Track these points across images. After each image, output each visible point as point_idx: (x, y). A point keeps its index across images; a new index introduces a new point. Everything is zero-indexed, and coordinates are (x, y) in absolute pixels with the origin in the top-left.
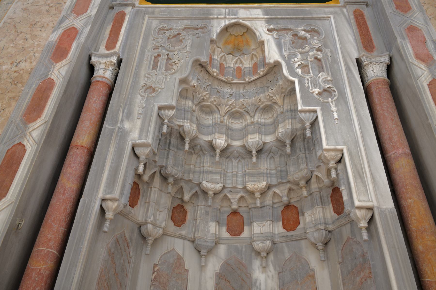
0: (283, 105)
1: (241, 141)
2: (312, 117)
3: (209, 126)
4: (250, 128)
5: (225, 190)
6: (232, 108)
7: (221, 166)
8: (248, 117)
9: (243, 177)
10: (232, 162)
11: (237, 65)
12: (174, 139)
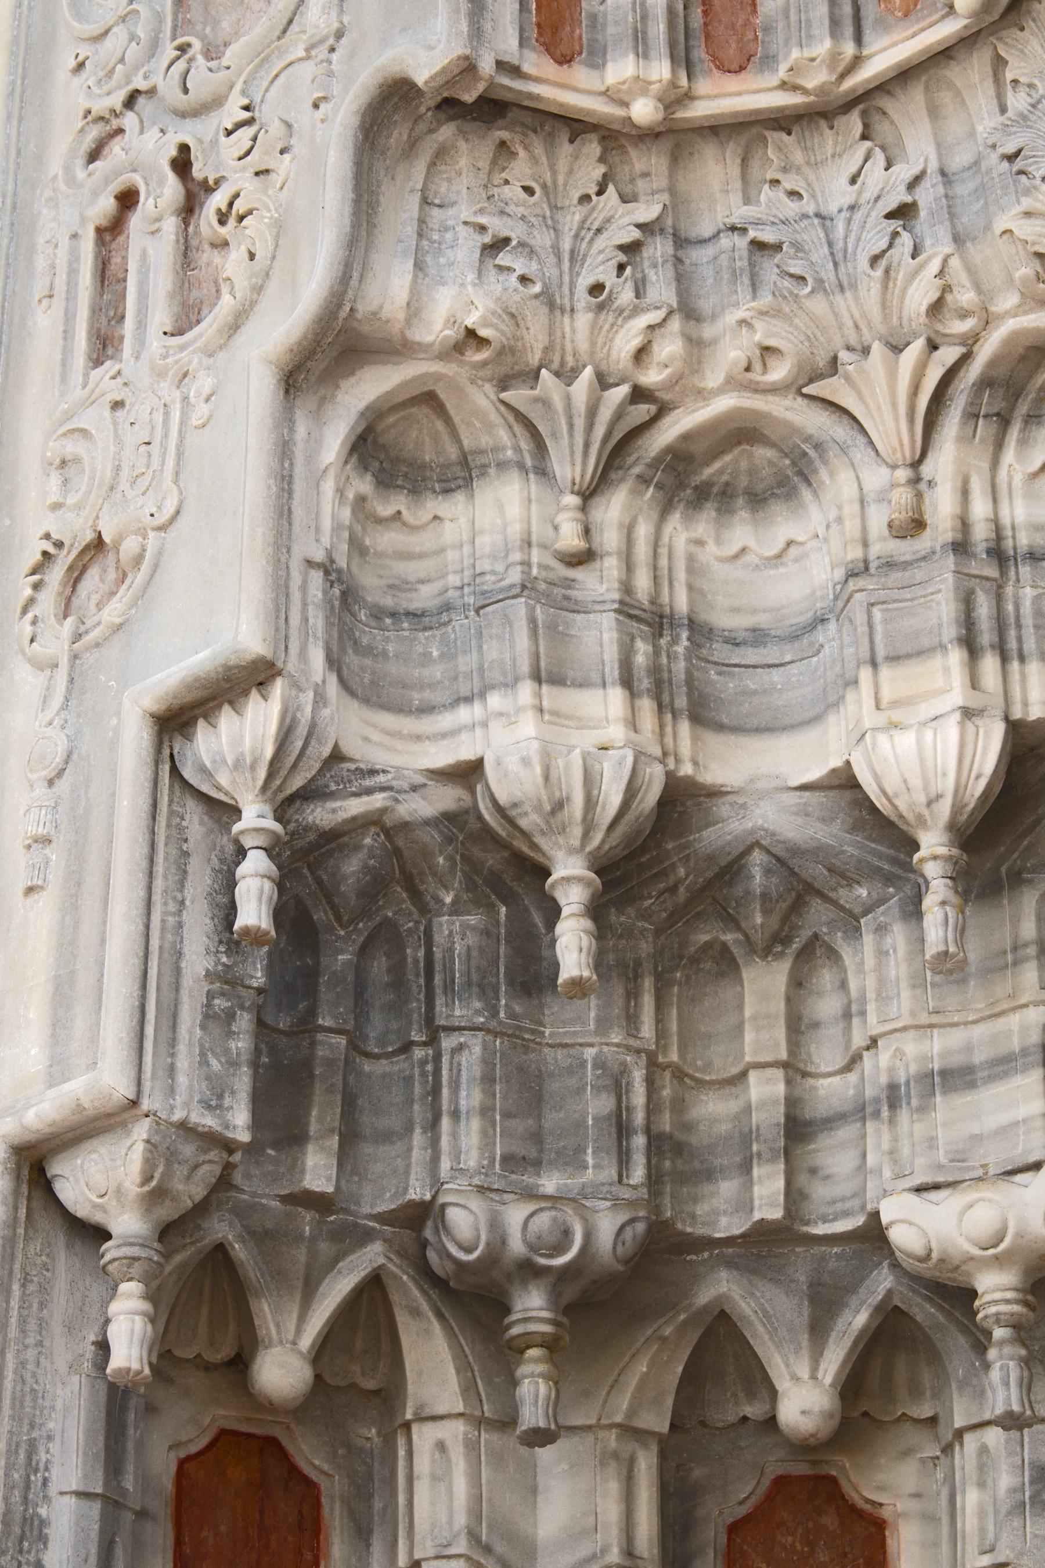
6: (970, 343)
12: (456, 910)
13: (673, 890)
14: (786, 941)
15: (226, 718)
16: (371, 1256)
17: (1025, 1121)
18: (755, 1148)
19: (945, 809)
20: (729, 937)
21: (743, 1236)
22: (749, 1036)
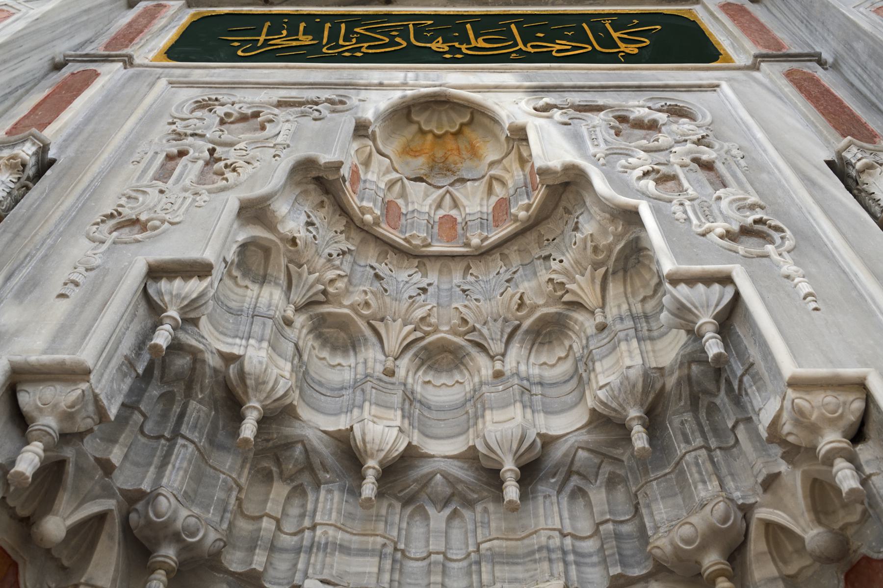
0: (603, 307)
1: (462, 438)
2: (719, 295)
4: (491, 393)
6: (427, 334)
7: (382, 525)
8: (482, 360)
9: (469, 574)
10: (427, 517)
11: (441, 213)
12: (200, 402)
13: (268, 441)
14: (292, 480)
15: (178, 283)
16: (109, 504)
17: (369, 573)
18: (259, 543)
19: (382, 455)
20: (274, 469)
21: (240, 574)
22: (269, 504)
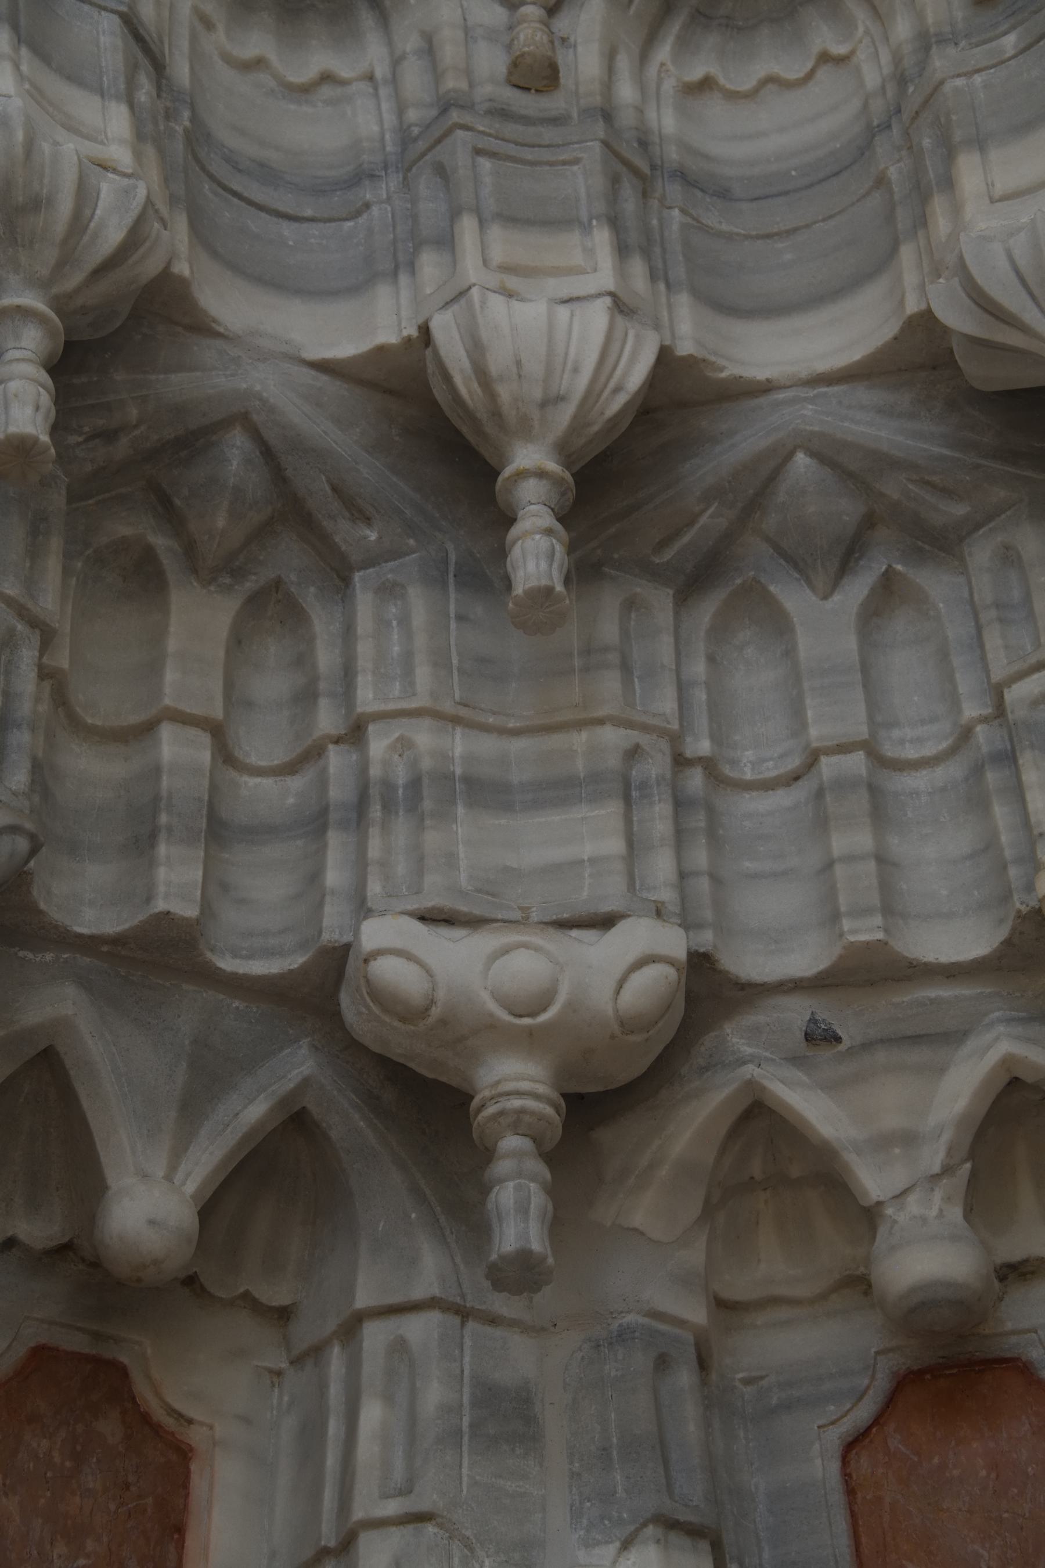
1: (873, 294)
3: (360, 177)
5: (736, 1036)
7: (610, 684)
9: (978, 803)
10: (779, 625)
13: (109, 436)
14: (238, 574)
17: (593, 861)
18: (163, 818)
19: (564, 416)
20: (161, 542)
21: (117, 941)
22: (171, 676)
